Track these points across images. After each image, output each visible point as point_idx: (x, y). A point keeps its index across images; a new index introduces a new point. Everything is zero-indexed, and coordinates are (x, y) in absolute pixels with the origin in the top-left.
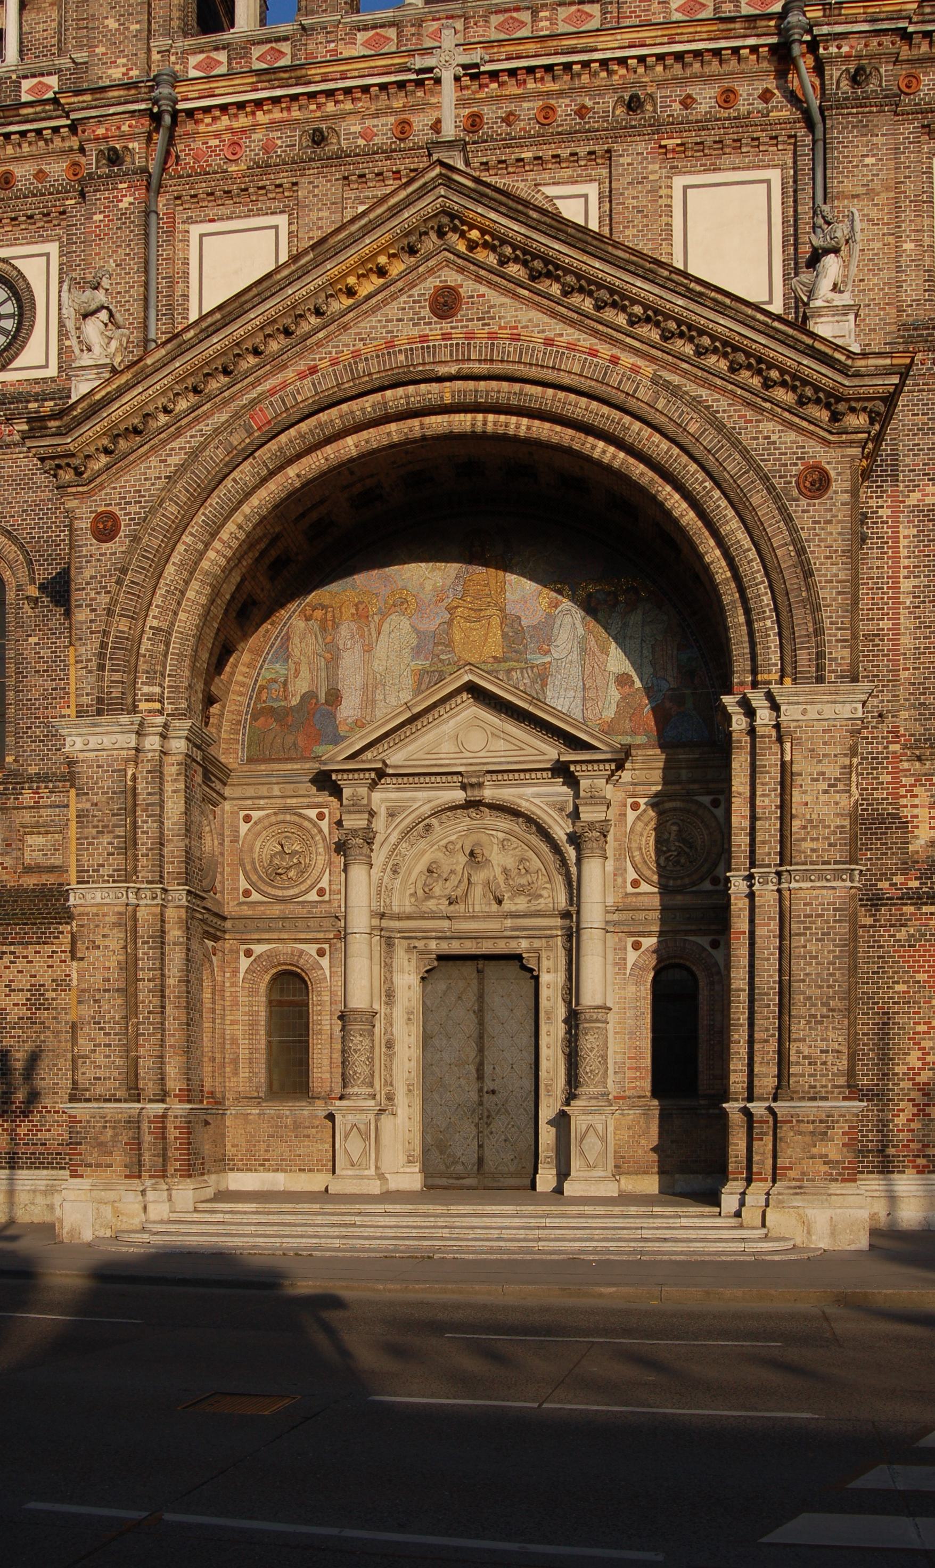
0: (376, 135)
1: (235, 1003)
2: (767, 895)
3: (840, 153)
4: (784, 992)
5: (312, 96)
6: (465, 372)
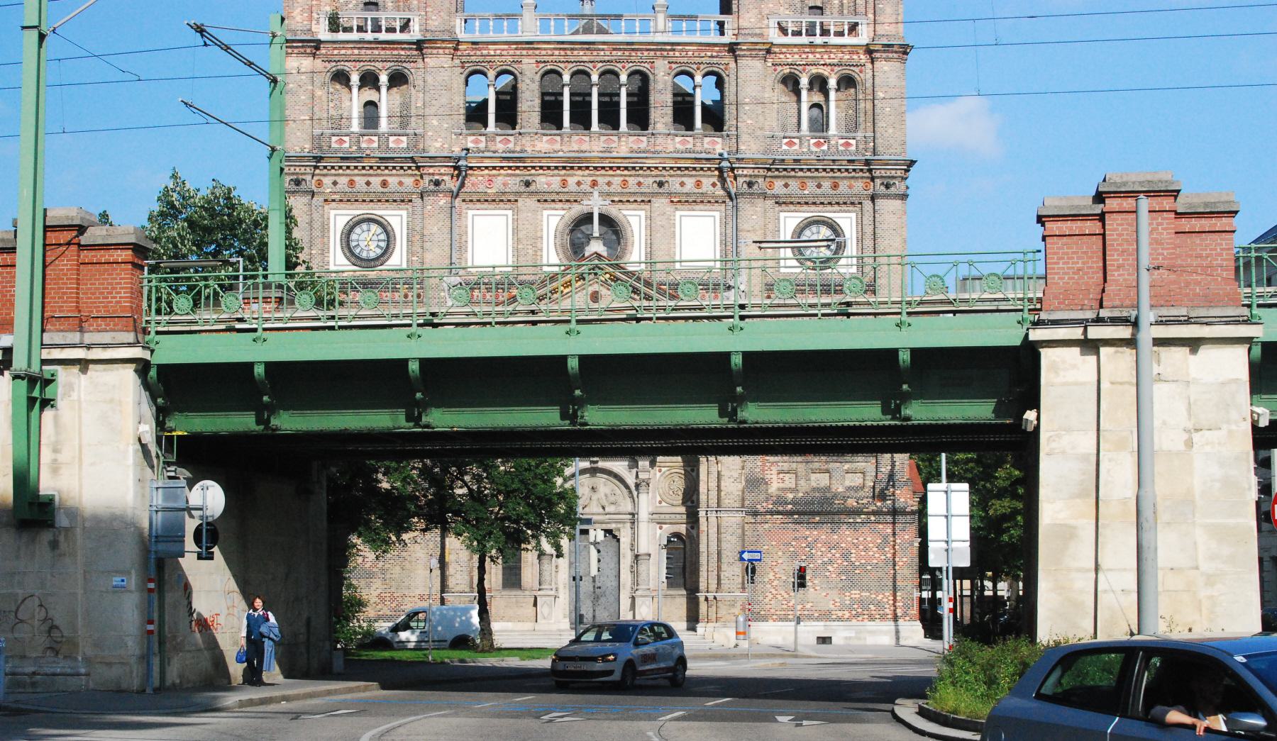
2: (713, 520)
4: (719, 553)
5: (525, 167)
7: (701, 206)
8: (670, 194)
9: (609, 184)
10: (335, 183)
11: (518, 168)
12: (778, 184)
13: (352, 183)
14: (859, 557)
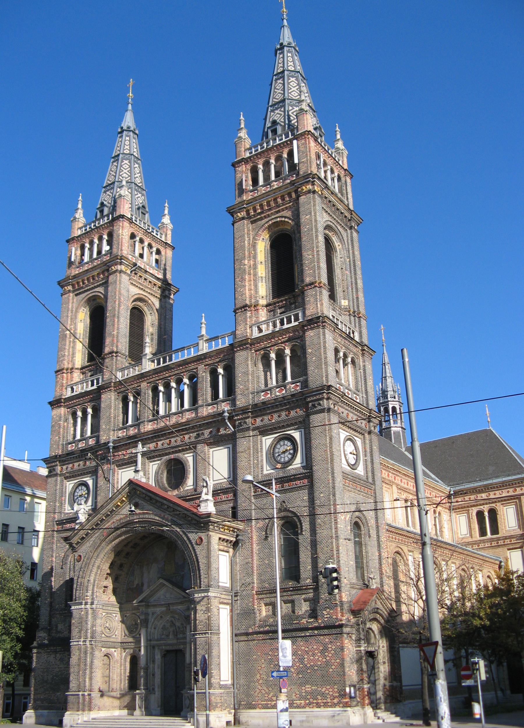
12: (258, 420)
14: (309, 659)
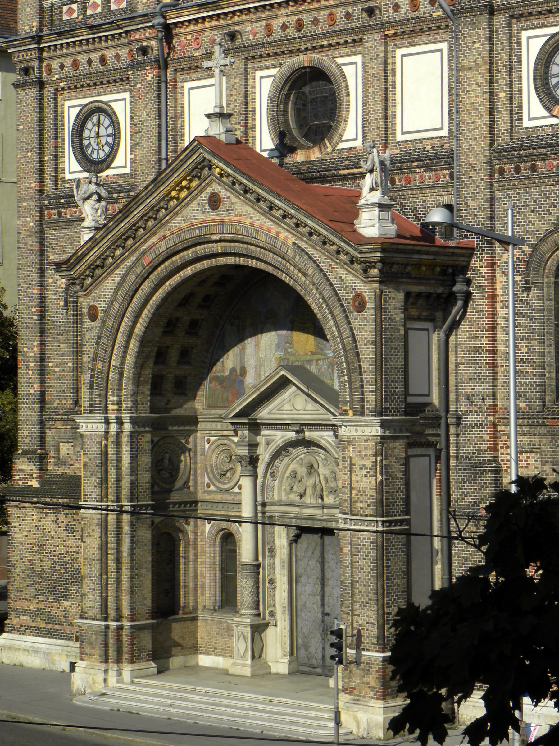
0: (257, 33)
1: (204, 552)
3: (463, 41)
6: (223, 238)
7: (423, 38)
8: (382, 26)
9: (315, 21)
10: (62, 67)
11: (218, 16)
13: (75, 64)
